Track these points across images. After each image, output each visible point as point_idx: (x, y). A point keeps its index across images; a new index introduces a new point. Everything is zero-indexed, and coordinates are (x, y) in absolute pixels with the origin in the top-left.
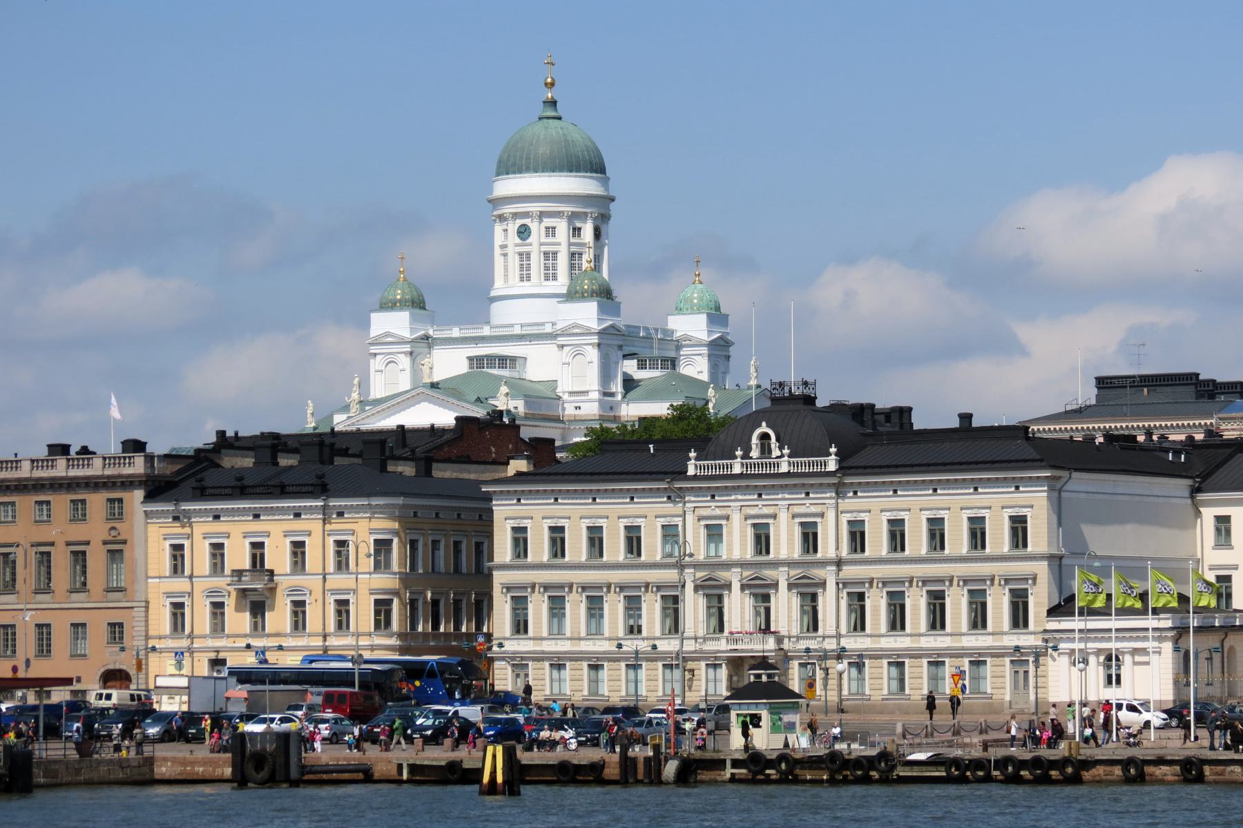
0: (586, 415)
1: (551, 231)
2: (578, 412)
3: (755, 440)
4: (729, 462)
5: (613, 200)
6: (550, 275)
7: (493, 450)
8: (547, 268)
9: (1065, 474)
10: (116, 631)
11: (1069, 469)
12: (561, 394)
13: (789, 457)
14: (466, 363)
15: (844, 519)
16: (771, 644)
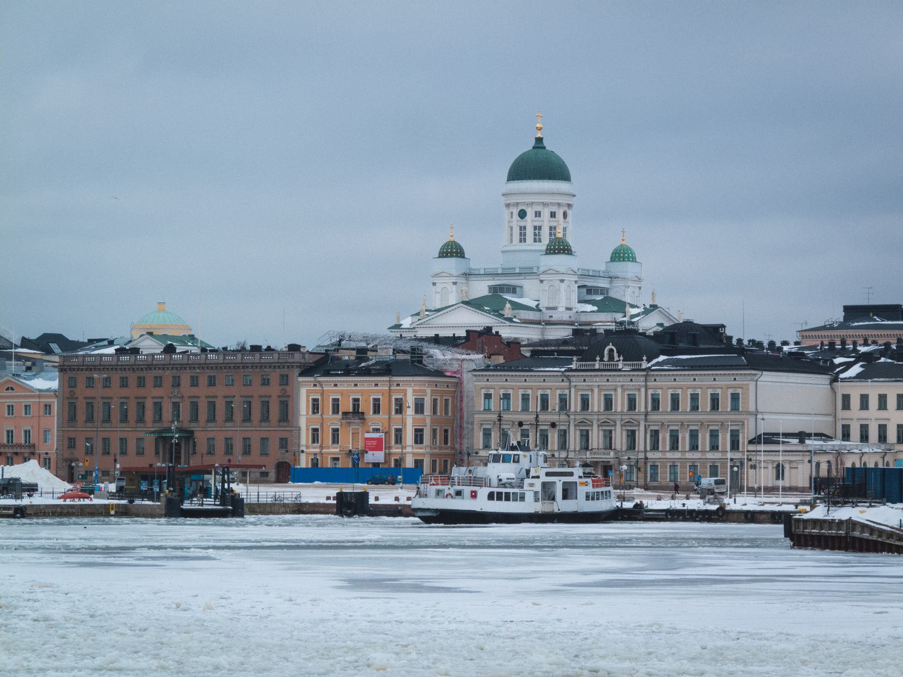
0: (555, 321)
1: (538, 214)
2: (551, 319)
3: (606, 352)
4: (593, 363)
5: (575, 196)
6: (537, 239)
7: (486, 348)
8: (535, 235)
9: (760, 373)
10: (284, 443)
11: (761, 370)
12: (541, 309)
13: (623, 361)
14: (487, 289)
15: (650, 392)
16: (612, 454)
